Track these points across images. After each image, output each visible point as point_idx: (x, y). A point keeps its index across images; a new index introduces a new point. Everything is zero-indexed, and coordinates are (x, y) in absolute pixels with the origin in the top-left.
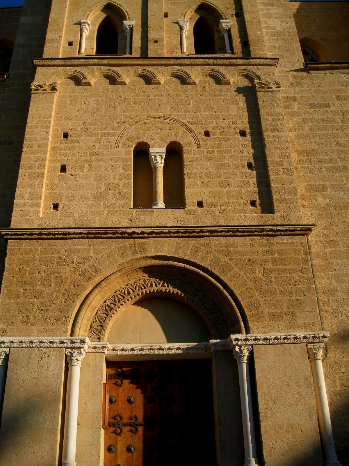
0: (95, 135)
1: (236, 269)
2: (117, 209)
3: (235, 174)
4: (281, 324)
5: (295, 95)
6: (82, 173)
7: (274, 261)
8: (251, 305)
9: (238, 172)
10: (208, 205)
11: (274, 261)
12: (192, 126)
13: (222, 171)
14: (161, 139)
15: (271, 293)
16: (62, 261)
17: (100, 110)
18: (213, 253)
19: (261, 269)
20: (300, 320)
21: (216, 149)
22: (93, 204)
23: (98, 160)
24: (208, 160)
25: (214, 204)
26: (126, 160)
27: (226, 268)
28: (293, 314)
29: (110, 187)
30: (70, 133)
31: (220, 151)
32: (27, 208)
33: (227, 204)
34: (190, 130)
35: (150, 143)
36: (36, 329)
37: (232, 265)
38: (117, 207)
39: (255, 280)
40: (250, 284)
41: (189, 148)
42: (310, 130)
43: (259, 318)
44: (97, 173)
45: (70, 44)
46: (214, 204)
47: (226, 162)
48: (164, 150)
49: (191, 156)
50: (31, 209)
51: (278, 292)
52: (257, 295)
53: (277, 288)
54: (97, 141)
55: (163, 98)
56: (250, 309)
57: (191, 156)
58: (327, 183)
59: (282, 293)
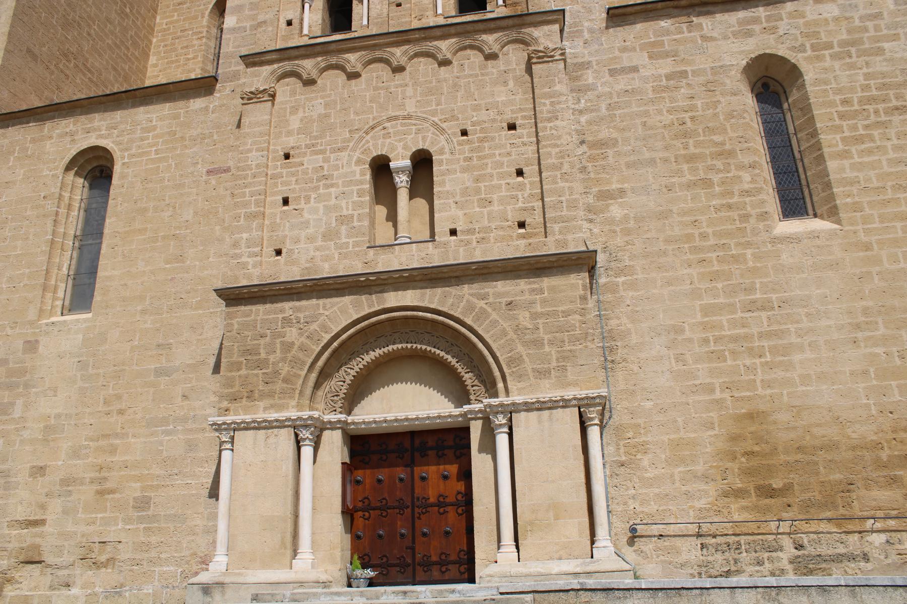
0: (322, 152)
1: (494, 316)
2: (351, 249)
3: (499, 187)
4: (546, 383)
5: (590, 59)
6: (308, 206)
7: (544, 302)
8: (511, 361)
9: (503, 182)
10: (463, 232)
11: (544, 302)
12: (444, 125)
13: (481, 185)
14: (405, 147)
15: (537, 343)
16: (287, 321)
17: (327, 116)
18: (467, 296)
19: (527, 315)
20: (571, 377)
21: (475, 155)
22: (322, 246)
23: (327, 186)
24: (464, 170)
25: (470, 231)
26: (362, 182)
27: (482, 315)
28: (564, 369)
29: (343, 220)
30: (292, 153)
31: (480, 157)
32: (244, 259)
33: (487, 230)
34: (442, 131)
36: (261, 404)
37: (489, 310)
38: (351, 246)
39: (517, 329)
40: (511, 335)
41: (441, 157)
42: (607, 109)
43: (520, 377)
44: (326, 203)
45: (289, 23)
46: (470, 231)
47: (489, 170)
48: (407, 163)
49: (444, 167)
50: (249, 260)
51: (546, 342)
52: (520, 348)
53: (546, 337)
54: (326, 160)
55: (408, 89)
56: (509, 366)
57: (444, 167)
58: (626, 185)
59: (551, 343)
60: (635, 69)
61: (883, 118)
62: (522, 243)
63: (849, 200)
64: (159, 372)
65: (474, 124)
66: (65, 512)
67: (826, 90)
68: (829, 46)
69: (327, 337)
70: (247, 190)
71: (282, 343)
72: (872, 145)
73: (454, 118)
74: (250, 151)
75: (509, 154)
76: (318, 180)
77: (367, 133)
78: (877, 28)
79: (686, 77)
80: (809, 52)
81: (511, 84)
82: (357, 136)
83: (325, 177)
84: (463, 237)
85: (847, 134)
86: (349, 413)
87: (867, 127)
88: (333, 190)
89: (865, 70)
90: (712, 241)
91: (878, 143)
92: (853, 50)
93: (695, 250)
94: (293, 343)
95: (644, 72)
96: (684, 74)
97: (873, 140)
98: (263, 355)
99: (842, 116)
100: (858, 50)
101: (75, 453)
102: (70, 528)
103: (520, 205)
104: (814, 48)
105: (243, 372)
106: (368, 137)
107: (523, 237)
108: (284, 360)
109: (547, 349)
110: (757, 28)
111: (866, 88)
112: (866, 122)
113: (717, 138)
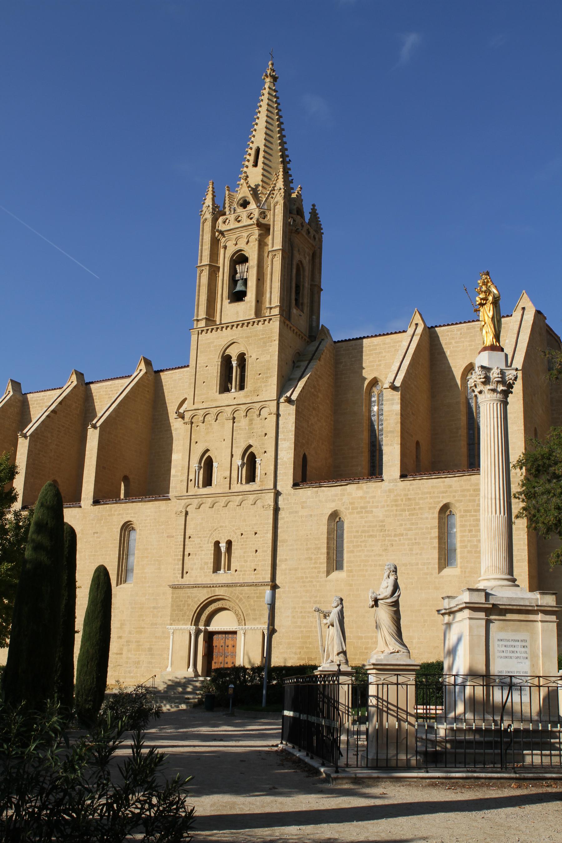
0: (200, 537)
7: (257, 597)
8: (247, 615)
12: (236, 531)
13: (245, 555)
15: (254, 610)
23: (202, 550)
24: (241, 549)
33: (245, 571)
34: (236, 533)
35: (220, 541)
40: (248, 607)
46: (241, 571)
48: (224, 544)
49: (235, 547)
52: (250, 611)
60: (297, 512)
61: (366, 539)
62: (253, 577)
63: (350, 568)
64: (154, 608)
65: (245, 531)
66: (128, 651)
67: (352, 527)
68: (357, 508)
69: (200, 603)
70: (177, 550)
71: (187, 604)
72: (361, 549)
73: (239, 529)
75: (254, 544)
76: (199, 548)
79: (311, 517)
81: (257, 516)
82: (210, 532)
83: (201, 547)
84: (239, 573)
85: (355, 544)
86: (209, 625)
87: (361, 542)
88: (203, 552)
90: (309, 579)
91: (363, 548)
92: (364, 511)
93: (303, 582)
94: (190, 604)
95: (300, 514)
96: (311, 515)
97: (361, 547)
98: (182, 608)
100: (365, 511)
101: (130, 633)
102: (130, 656)
103: (255, 563)
104: (353, 509)
105: (176, 612)
107: (255, 574)
108: (187, 609)
109: (257, 612)
110: (337, 498)
111: (364, 526)
112: (361, 540)
113: (317, 542)
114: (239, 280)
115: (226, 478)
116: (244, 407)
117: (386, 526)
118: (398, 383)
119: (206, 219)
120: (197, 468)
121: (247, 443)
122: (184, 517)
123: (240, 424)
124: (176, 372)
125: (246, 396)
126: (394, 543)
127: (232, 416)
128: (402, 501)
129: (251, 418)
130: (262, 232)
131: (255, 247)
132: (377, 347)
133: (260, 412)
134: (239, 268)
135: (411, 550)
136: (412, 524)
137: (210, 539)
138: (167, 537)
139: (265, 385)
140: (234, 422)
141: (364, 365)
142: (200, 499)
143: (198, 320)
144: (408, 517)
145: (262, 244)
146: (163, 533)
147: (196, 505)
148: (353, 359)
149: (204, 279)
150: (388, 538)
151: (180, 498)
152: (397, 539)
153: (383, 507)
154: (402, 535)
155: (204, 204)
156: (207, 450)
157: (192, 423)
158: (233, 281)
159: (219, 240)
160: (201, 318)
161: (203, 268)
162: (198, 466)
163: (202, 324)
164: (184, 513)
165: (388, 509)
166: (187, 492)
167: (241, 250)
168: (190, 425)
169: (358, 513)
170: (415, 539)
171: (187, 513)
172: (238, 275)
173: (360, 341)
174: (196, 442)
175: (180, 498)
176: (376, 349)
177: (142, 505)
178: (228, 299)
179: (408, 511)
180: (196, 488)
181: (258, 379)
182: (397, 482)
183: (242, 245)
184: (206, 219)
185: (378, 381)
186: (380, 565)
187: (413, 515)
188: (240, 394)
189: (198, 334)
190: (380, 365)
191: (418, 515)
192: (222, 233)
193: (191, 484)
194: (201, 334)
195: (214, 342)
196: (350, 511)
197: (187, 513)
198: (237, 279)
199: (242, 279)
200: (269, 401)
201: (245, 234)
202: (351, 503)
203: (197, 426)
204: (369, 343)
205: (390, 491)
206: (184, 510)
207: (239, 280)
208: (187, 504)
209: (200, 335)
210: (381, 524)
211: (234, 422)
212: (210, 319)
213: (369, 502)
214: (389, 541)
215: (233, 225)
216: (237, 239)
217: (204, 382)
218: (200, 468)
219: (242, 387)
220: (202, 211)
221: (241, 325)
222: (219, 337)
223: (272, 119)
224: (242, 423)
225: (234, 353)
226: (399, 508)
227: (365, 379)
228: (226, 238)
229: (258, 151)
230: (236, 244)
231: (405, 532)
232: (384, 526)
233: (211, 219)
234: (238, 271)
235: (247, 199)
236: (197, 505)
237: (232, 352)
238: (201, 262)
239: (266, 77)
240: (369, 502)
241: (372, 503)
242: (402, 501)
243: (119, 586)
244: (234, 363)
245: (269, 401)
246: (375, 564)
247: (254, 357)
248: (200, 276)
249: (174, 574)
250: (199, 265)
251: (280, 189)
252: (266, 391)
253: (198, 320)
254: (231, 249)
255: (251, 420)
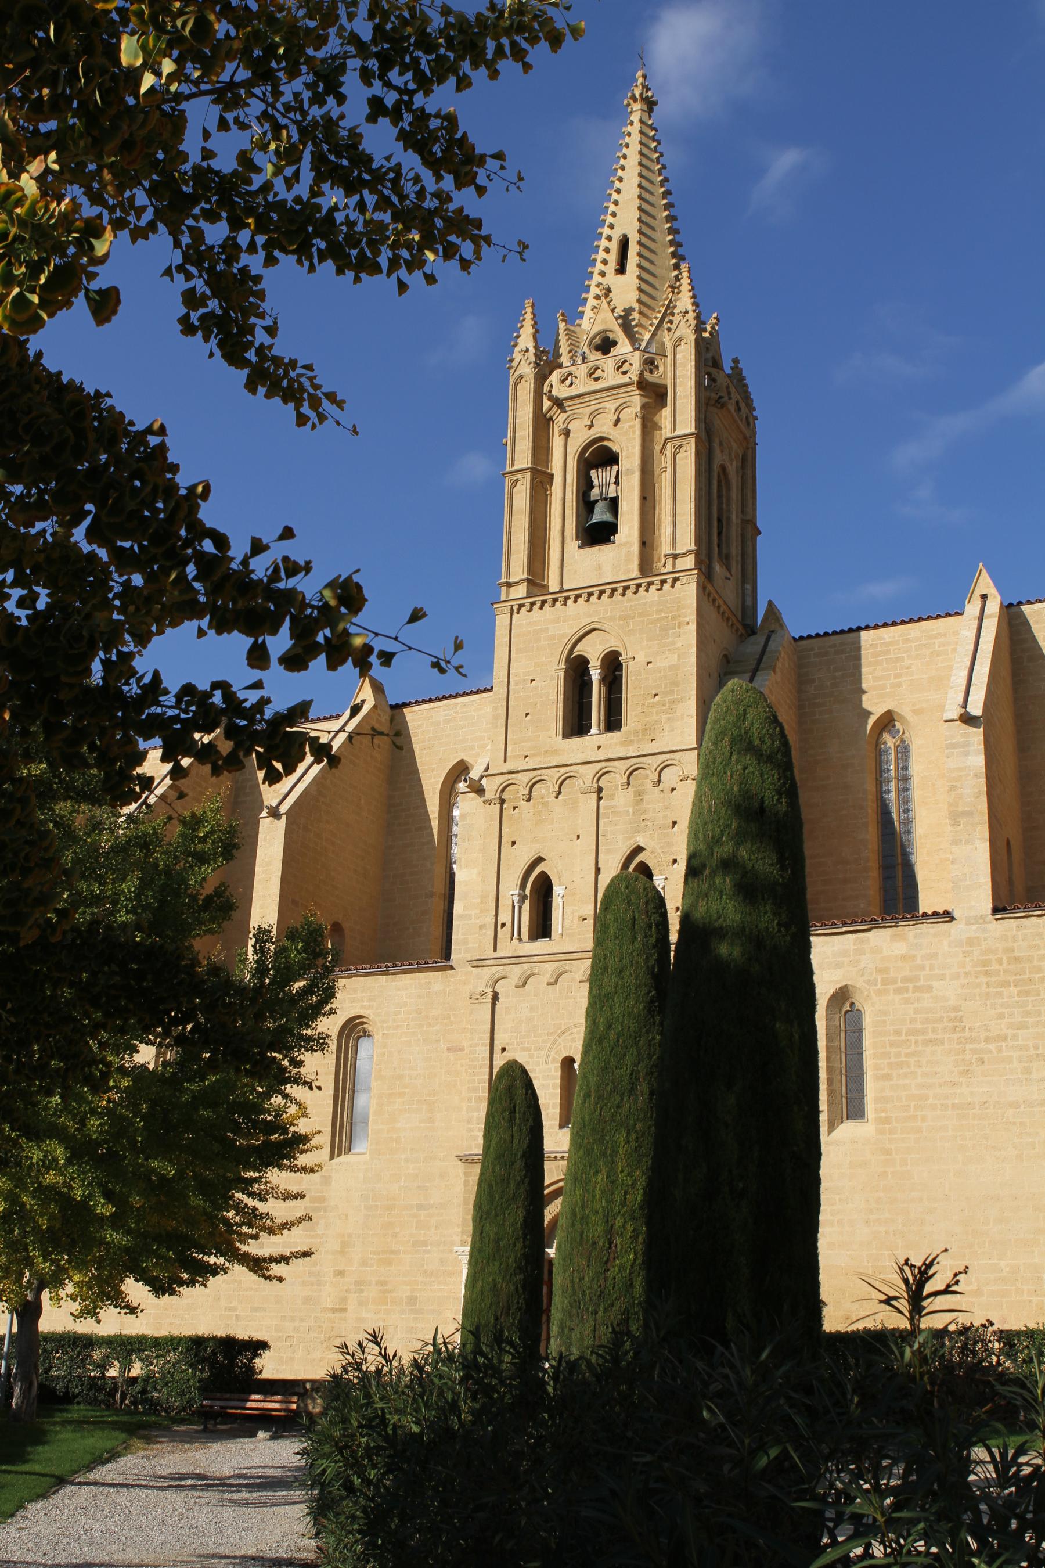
0: (528, 1049)
61: (920, 1048)
63: (883, 1115)
64: (420, 1207)
66: (361, 1304)
67: (884, 1021)
70: (476, 1078)
74: (477, 1045)
77: (559, 1036)
78: (932, 968)
80: (879, 986)
82: (552, 1038)
85: (893, 1060)
87: (907, 1055)
89: (916, 1005)
92: (911, 986)
99: (892, 1044)
101: (364, 1263)
102: (364, 1315)
104: (885, 982)
106: (560, 1040)
111: (913, 1021)
112: (908, 1051)
114: (597, 501)
115: (585, 919)
116: (622, 766)
117: (964, 1019)
118: (976, 708)
119: (521, 377)
120: (516, 899)
121: (632, 842)
122: (490, 1005)
123: (613, 803)
124: (439, 707)
125: (626, 743)
126: (985, 1057)
127: (595, 785)
128: (1001, 964)
129: (640, 788)
130: (647, 400)
131: (634, 432)
132: (892, 648)
133: (660, 776)
134: (597, 476)
135: (1027, 1071)
136: (1028, 1014)
137: (552, 1054)
138: (448, 1049)
139: (669, 719)
140: (600, 799)
141: (864, 686)
142: (526, 966)
143: (509, 585)
144: (1016, 999)
145: (648, 426)
146: (438, 1041)
147: (516, 979)
148: (837, 674)
149: (521, 497)
150: (972, 1046)
151: (480, 963)
152: (992, 1047)
153: (957, 976)
154: (1004, 1038)
155: (515, 345)
156: (540, 860)
157: (502, 801)
158: (586, 505)
159: (551, 419)
160: (516, 580)
161: (519, 476)
162: (519, 895)
163: (520, 591)
164: (490, 995)
165: (967, 981)
166: (495, 950)
167: (602, 439)
168: (498, 806)
169: (898, 991)
170: (1037, 1048)
171: (495, 997)
172: (595, 493)
173: (852, 635)
174: (514, 843)
175: (480, 963)
176: (888, 652)
177: (387, 981)
178: (577, 539)
179: (1015, 986)
180: (515, 941)
181: (653, 705)
182: (985, 922)
183: (603, 427)
184: (521, 377)
185: (894, 720)
186: (954, 1106)
187: (1027, 993)
188: (612, 738)
189: (512, 614)
190: (899, 685)
191: (1039, 995)
192: (558, 403)
193: (504, 934)
194: (518, 613)
195: (547, 629)
196: (879, 986)
197: (495, 997)
198: (592, 499)
199: (606, 499)
200: (680, 751)
201: (611, 406)
202: (880, 971)
203: (515, 808)
204: (873, 640)
205: (971, 942)
206: (489, 990)
207: (597, 501)
208: (497, 976)
209: (515, 615)
210: (953, 1015)
211: (600, 799)
212: (536, 581)
213: (923, 968)
214: (974, 1051)
215: (582, 385)
216: (593, 415)
217: (527, 714)
218: (523, 898)
219: (613, 722)
220: (512, 361)
221: (608, 592)
222: (559, 618)
223: (652, 182)
224: (619, 800)
225: (593, 651)
226: (993, 979)
227: (869, 714)
228: (569, 413)
229: (624, 244)
230: (591, 426)
231: (1010, 1032)
232: (961, 1020)
233: (532, 376)
234: (596, 482)
235: (611, 336)
236: (520, 979)
237: (589, 649)
238: (513, 465)
239: (631, 102)
240: (923, 968)
241: (930, 970)
242: (1001, 964)
243: (336, 1160)
244: (595, 674)
245: (680, 751)
246: (942, 1105)
247: (641, 658)
248: (511, 494)
249: (470, 1130)
250: (508, 469)
251: (686, 312)
252: (672, 730)
253: (509, 585)
254: (580, 437)
255: (639, 794)
